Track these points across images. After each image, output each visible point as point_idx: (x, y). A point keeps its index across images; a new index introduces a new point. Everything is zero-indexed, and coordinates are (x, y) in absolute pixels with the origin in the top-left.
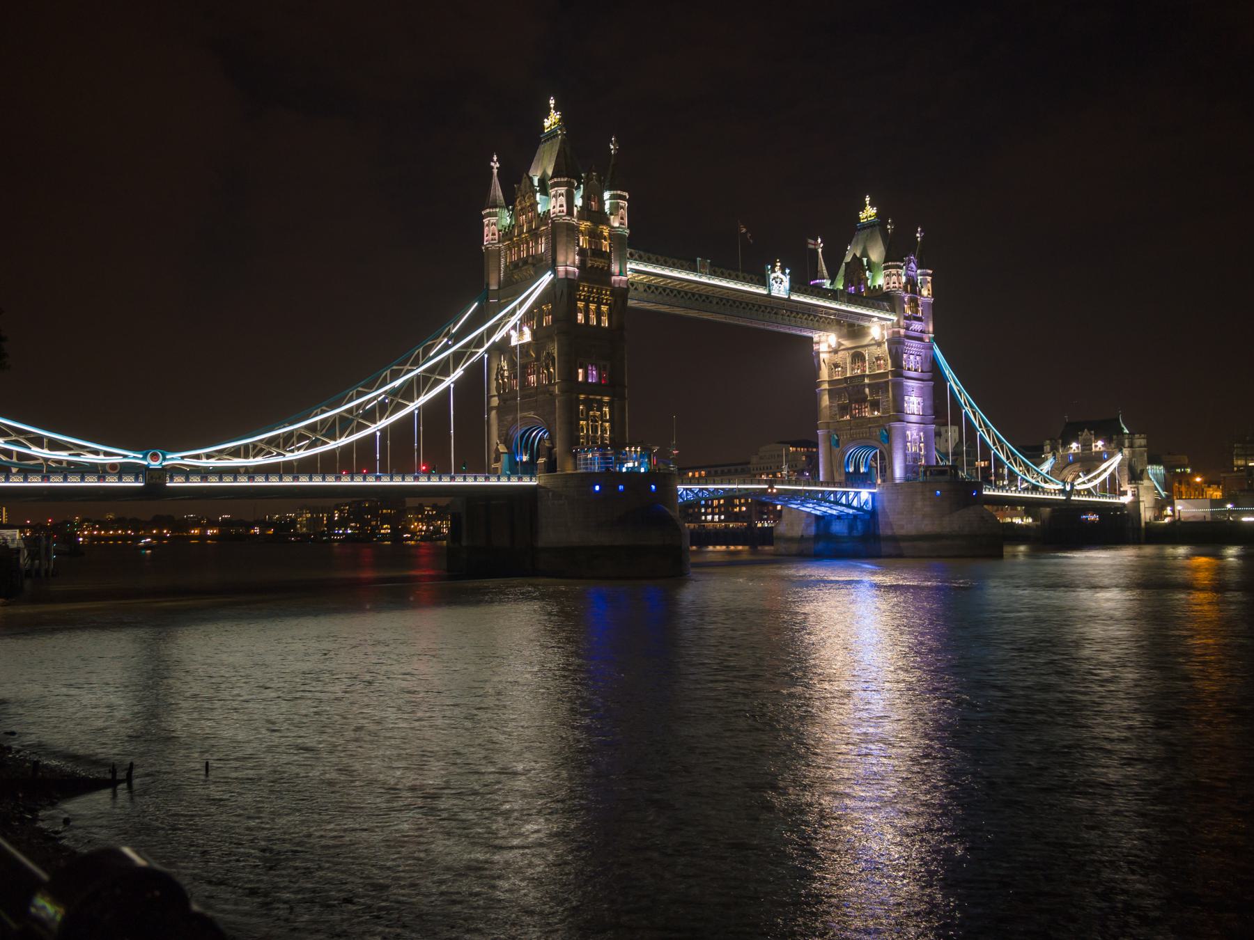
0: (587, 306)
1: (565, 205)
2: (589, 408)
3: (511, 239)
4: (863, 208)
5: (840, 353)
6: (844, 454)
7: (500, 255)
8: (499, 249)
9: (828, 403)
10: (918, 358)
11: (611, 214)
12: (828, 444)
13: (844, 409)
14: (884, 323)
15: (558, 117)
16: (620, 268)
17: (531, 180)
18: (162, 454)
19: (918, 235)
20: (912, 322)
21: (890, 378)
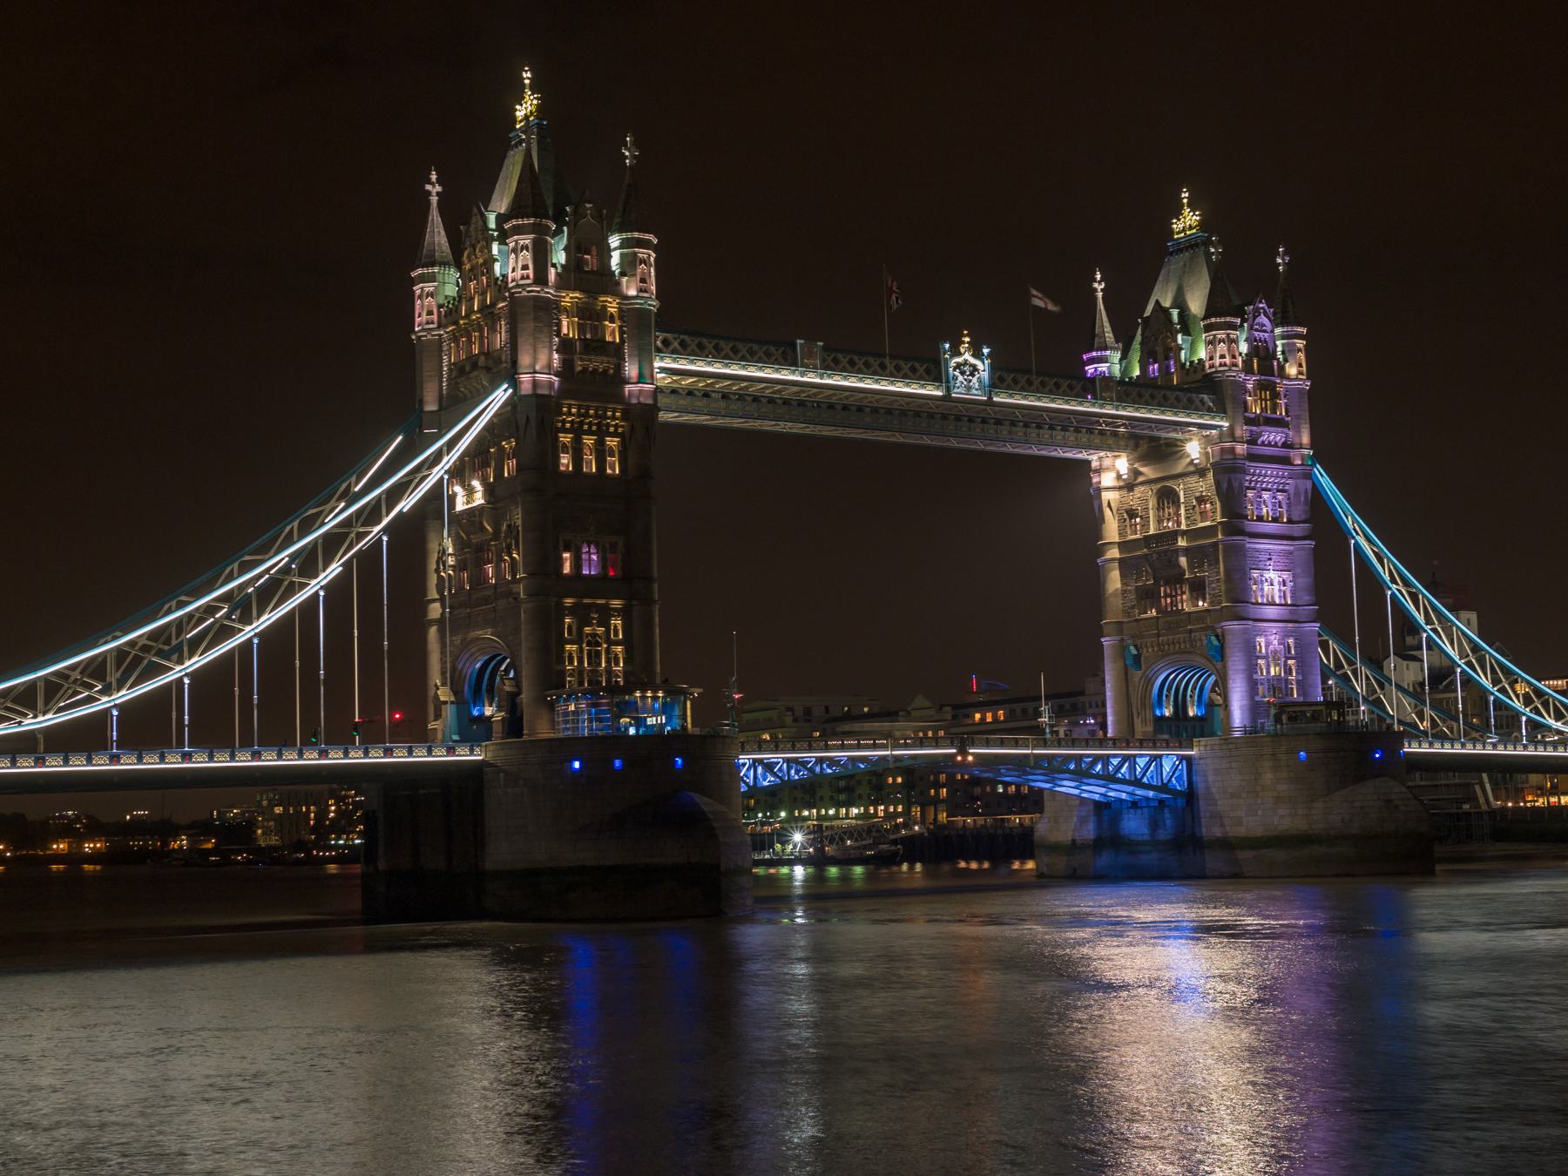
0: (577, 442)
1: (531, 266)
2: (584, 621)
3: (456, 323)
4: (1178, 214)
5: (1139, 491)
6: (1149, 682)
7: (441, 350)
8: (440, 340)
9: (1119, 585)
10: (1280, 496)
11: (623, 274)
15: (535, 102)
16: (640, 369)
17: (485, 221)
20: (1262, 428)
21: (1220, 537)
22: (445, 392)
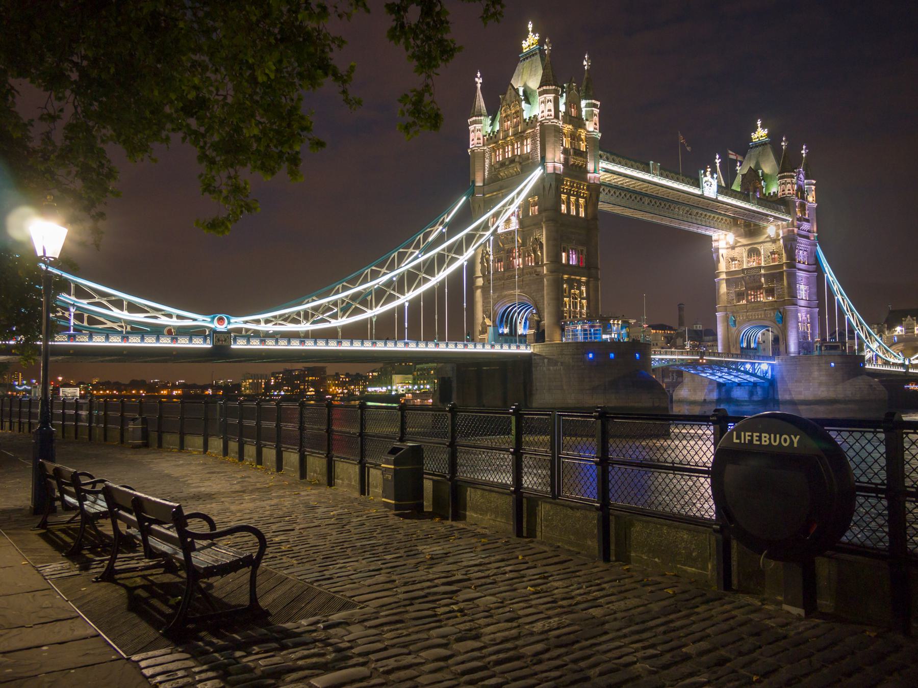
0: (568, 199)
1: (553, 110)
2: (571, 287)
3: (496, 142)
4: (755, 129)
5: (737, 250)
6: (739, 332)
7: (484, 157)
8: (484, 152)
12: (726, 324)
13: (740, 296)
14: (780, 223)
15: (537, 38)
18: (227, 318)
19: (803, 152)
21: (785, 268)
22: (486, 177)
